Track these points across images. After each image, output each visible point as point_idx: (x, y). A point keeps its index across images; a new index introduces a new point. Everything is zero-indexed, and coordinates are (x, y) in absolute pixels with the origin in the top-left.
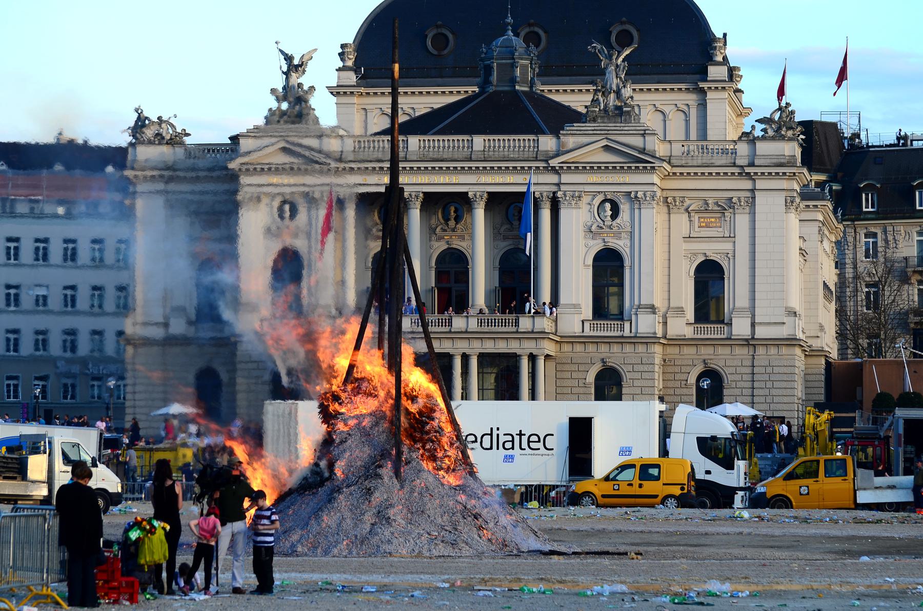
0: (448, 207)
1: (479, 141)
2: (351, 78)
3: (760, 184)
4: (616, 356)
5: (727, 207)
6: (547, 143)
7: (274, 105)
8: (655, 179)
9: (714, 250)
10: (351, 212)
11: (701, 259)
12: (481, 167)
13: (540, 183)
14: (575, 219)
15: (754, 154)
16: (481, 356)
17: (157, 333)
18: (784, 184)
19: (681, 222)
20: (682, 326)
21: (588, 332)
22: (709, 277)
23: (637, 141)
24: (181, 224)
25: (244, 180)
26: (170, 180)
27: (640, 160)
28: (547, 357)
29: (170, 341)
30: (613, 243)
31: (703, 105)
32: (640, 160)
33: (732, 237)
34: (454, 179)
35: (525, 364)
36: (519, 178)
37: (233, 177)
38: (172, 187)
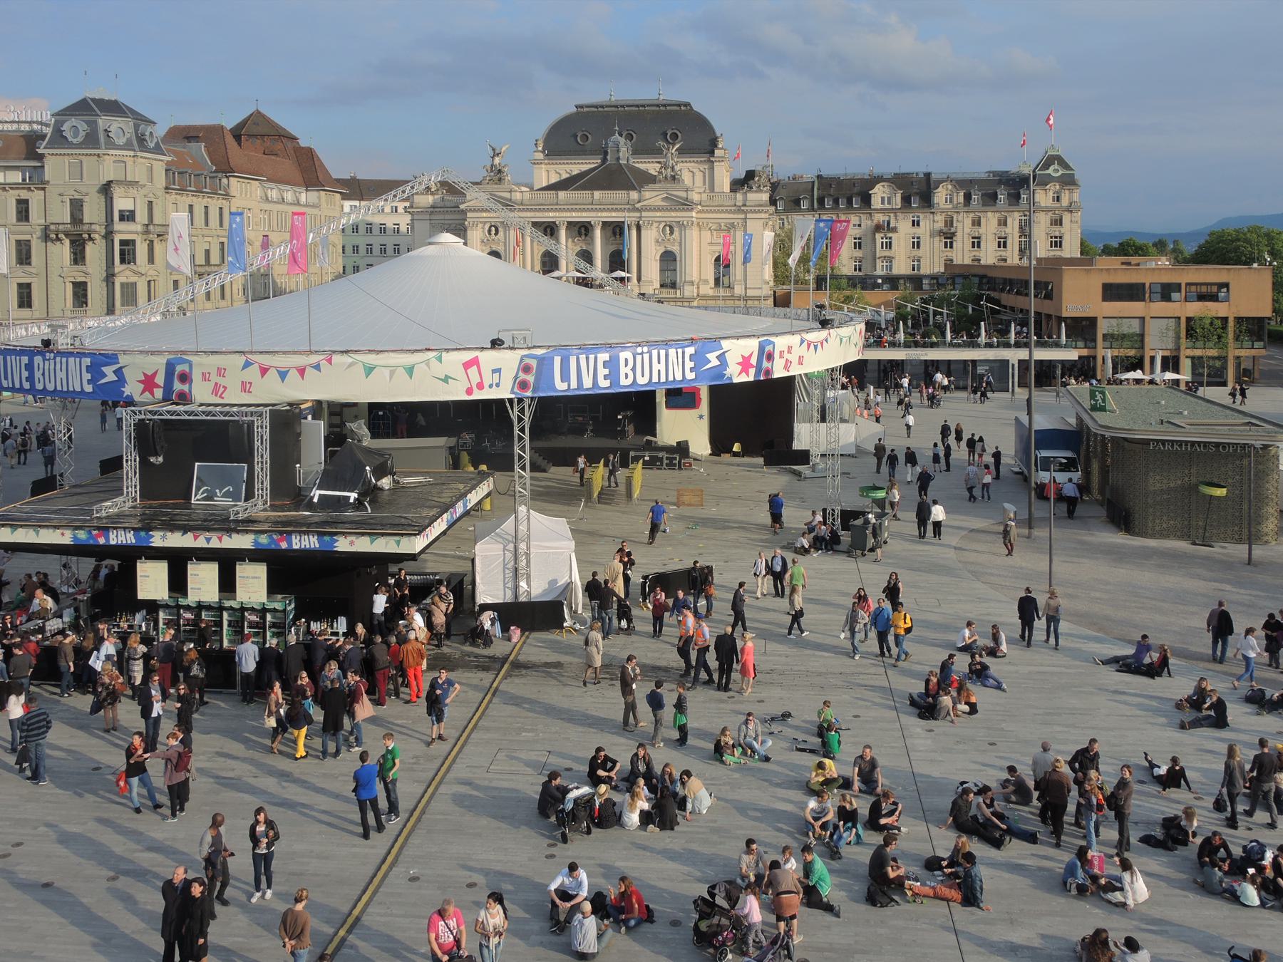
0: (583, 230)
1: (597, 194)
3: (749, 216)
5: (731, 227)
6: (634, 195)
8: (694, 214)
12: (600, 207)
13: (628, 218)
14: (650, 235)
15: (745, 200)
18: (763, 215)
19: (706, 235)
20: (708, 289)
22: (722, 264)
23: (683, 194)
25: (469, 215)
26: (432, 213)
27: (686, 204)
30: (670, 248)
31: (712, 169)
32: (686, 204)
34: (584, 214)
36: (620, 214)
37: (464, 212)
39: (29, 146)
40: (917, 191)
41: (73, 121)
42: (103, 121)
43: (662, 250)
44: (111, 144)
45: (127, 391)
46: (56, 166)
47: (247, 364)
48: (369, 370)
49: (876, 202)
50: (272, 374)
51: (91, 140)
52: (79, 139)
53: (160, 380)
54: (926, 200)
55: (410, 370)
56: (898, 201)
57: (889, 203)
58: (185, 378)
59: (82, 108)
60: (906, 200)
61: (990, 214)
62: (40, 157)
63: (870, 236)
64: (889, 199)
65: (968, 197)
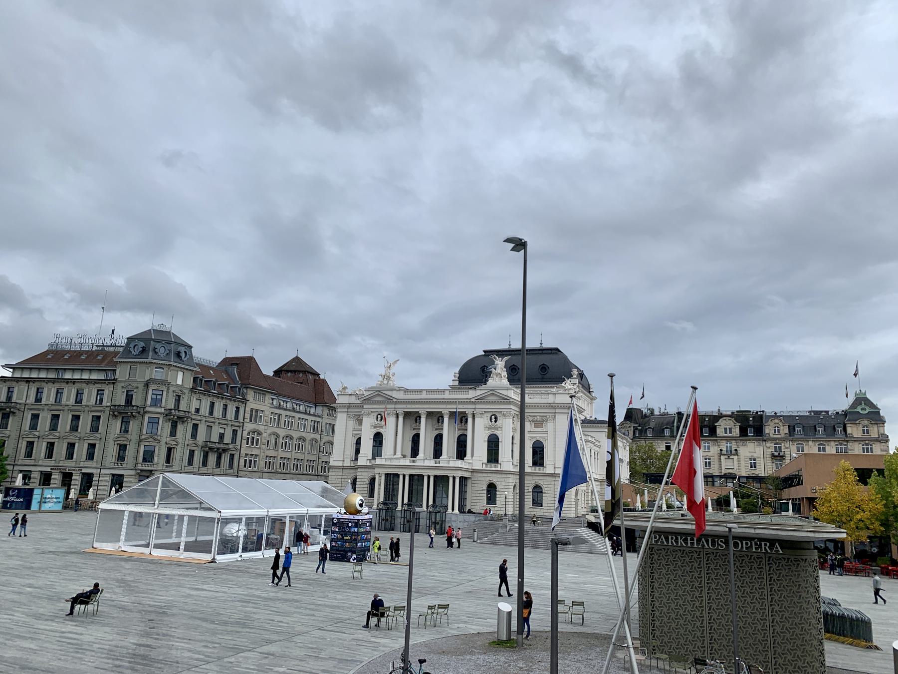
0: (436, 417)
2: (457, 383)
4: (496, 480)
7: (381, 379)
9: (538, 437)
10: (401, 419)
11: (534, 440)
16: (435, 477)
17: (340, 464)
21: (484, 468)
24: (352, 423)
26: (349, 407)
28: (461, 478)
29: (343, 468)
33: (546, 432)
35: (451, 480)
38: (350, 410)
40: (751, 425)
43: (489, 433)
49: (720, 432)
54: (759, 432)
56: (736, 432)
57: (730, 432)
60: (743, 432)
61: (811, 443)
63: (717, 457)
64: (730, 429)
65: (792, 429)
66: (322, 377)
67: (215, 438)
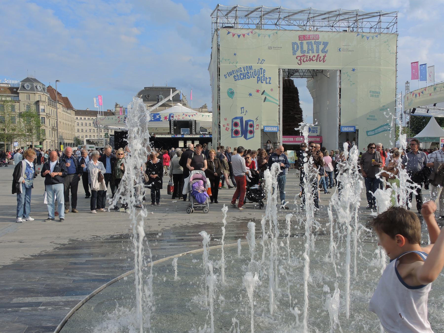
39: (14, 91)
41: (27, 84)
42: (35, 84)
44: (38, 91)
45: (161, 119)
46: (22, 96)
47: (183, 114)
48: (203, 116)
50: (188, 116)
51: (32, 89)
52: (29, 89)
53: (168, 117)
55: (209, 116)
58: (172, 117)
59: (27, 80)
62: (18, 93)
66: (63, 96)
67: (53, 126)
